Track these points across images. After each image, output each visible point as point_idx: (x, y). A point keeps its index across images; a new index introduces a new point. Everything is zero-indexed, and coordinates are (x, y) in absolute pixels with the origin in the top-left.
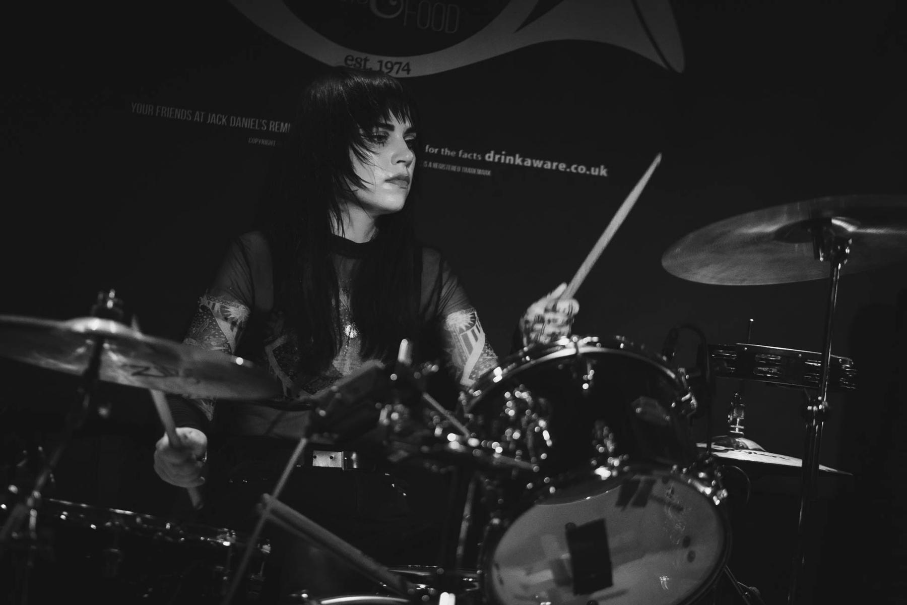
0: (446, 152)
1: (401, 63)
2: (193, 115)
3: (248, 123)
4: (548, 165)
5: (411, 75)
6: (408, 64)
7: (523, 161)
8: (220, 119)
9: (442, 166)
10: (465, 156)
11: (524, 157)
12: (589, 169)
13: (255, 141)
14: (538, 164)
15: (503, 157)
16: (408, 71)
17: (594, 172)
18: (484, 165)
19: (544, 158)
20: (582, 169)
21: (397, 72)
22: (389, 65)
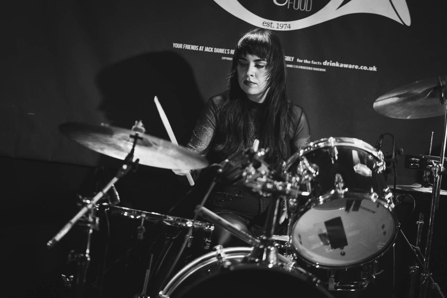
0: (306, 61)
2: (199, 48)
3: (221, 51)
4: (350, 66)
8: (210, 50)
9: (304, 68)
10: (315, 63)
11: (340, 63)
12: (368, 68)
13: (224, 58)
15: (331, 63)
16: (290, 27)
17: (371, 69)
18: (322, 67)
19: (348, 63)
20: (365, 68)
22: (282, 25)
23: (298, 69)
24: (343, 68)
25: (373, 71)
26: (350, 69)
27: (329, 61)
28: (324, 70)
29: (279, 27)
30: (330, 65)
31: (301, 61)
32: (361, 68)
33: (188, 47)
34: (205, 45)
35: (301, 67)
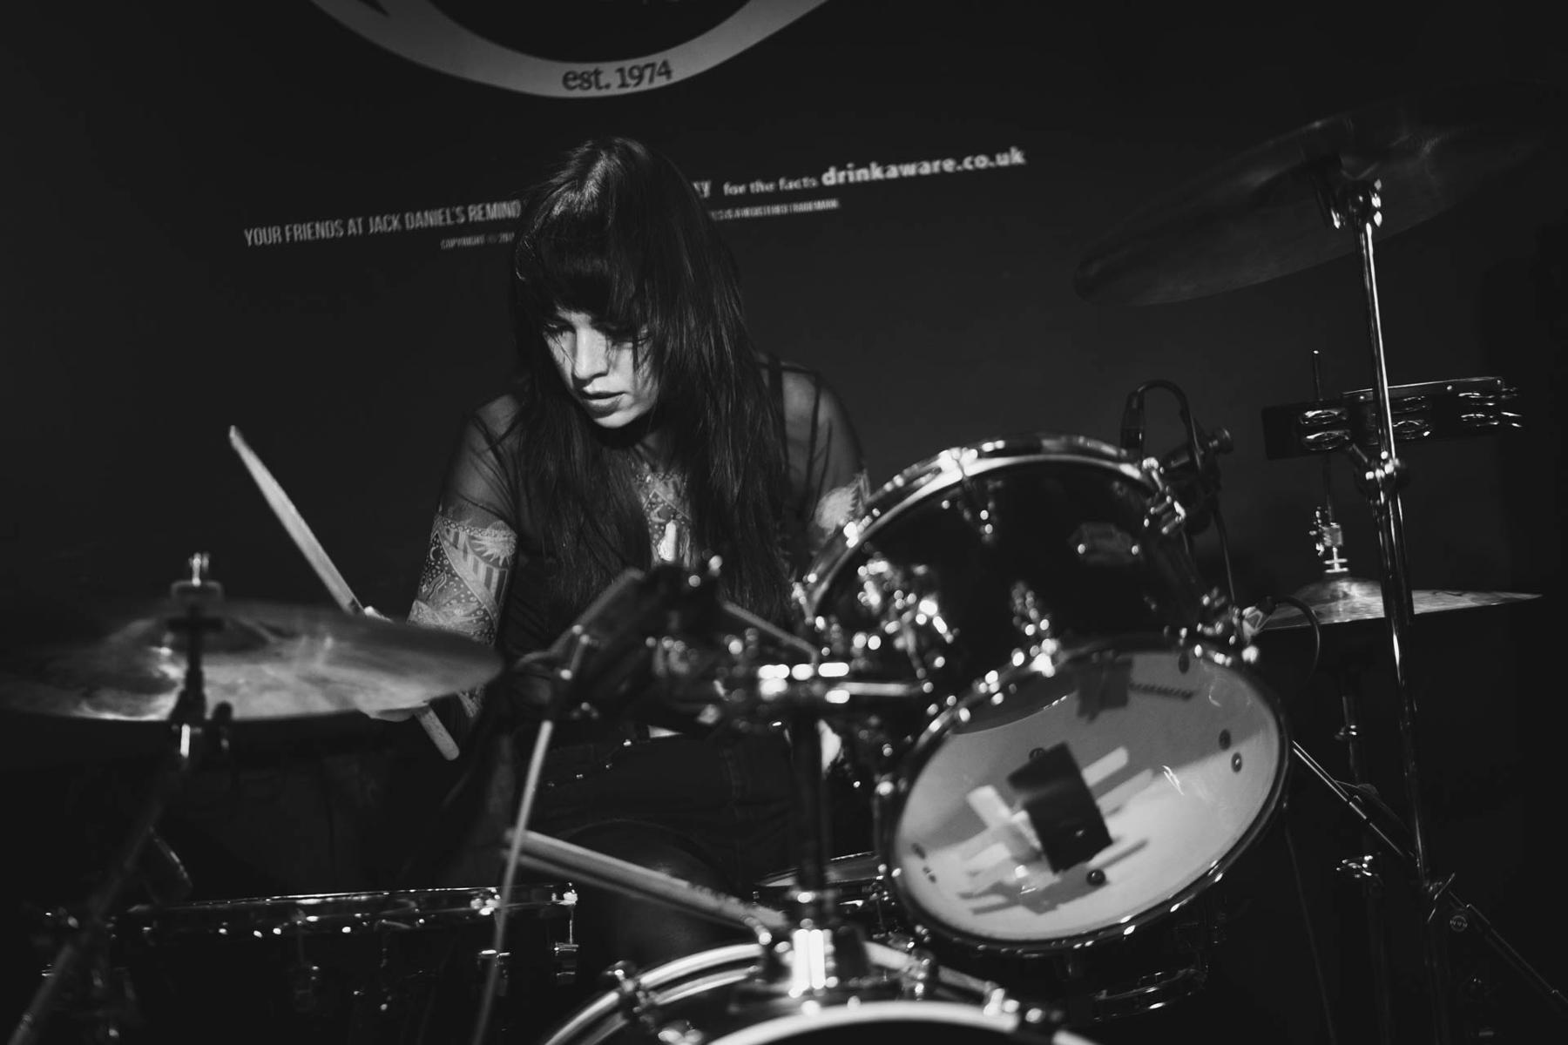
0: (758, 187)
1: (653, 65)
2: (345, 226)
3: (433, 218)
4: (926, 169)
5: (672, 81)
6: (665, 64)
7: (885, 171)
8: (390, 223)
9: (757, 212)
10: (793, 185)
11: (884, 164)
12: (993, 159)
13: (451, 243)
14: (909, 170)
15: (851, 174)
16: (668, 73)
17: (1003, 160)
18: (823, 192)
20: (982, 162)
21: (651, 80)
22: (636, 73)
23: (735, 220)
24: (901, 179)
25: (1013, 168)
26: (926, 177)
29: (629, 81)
30: (851, 179)
32: (967, 164)
33: (303, 232)
34: (367, 213)
35: (746, 212)
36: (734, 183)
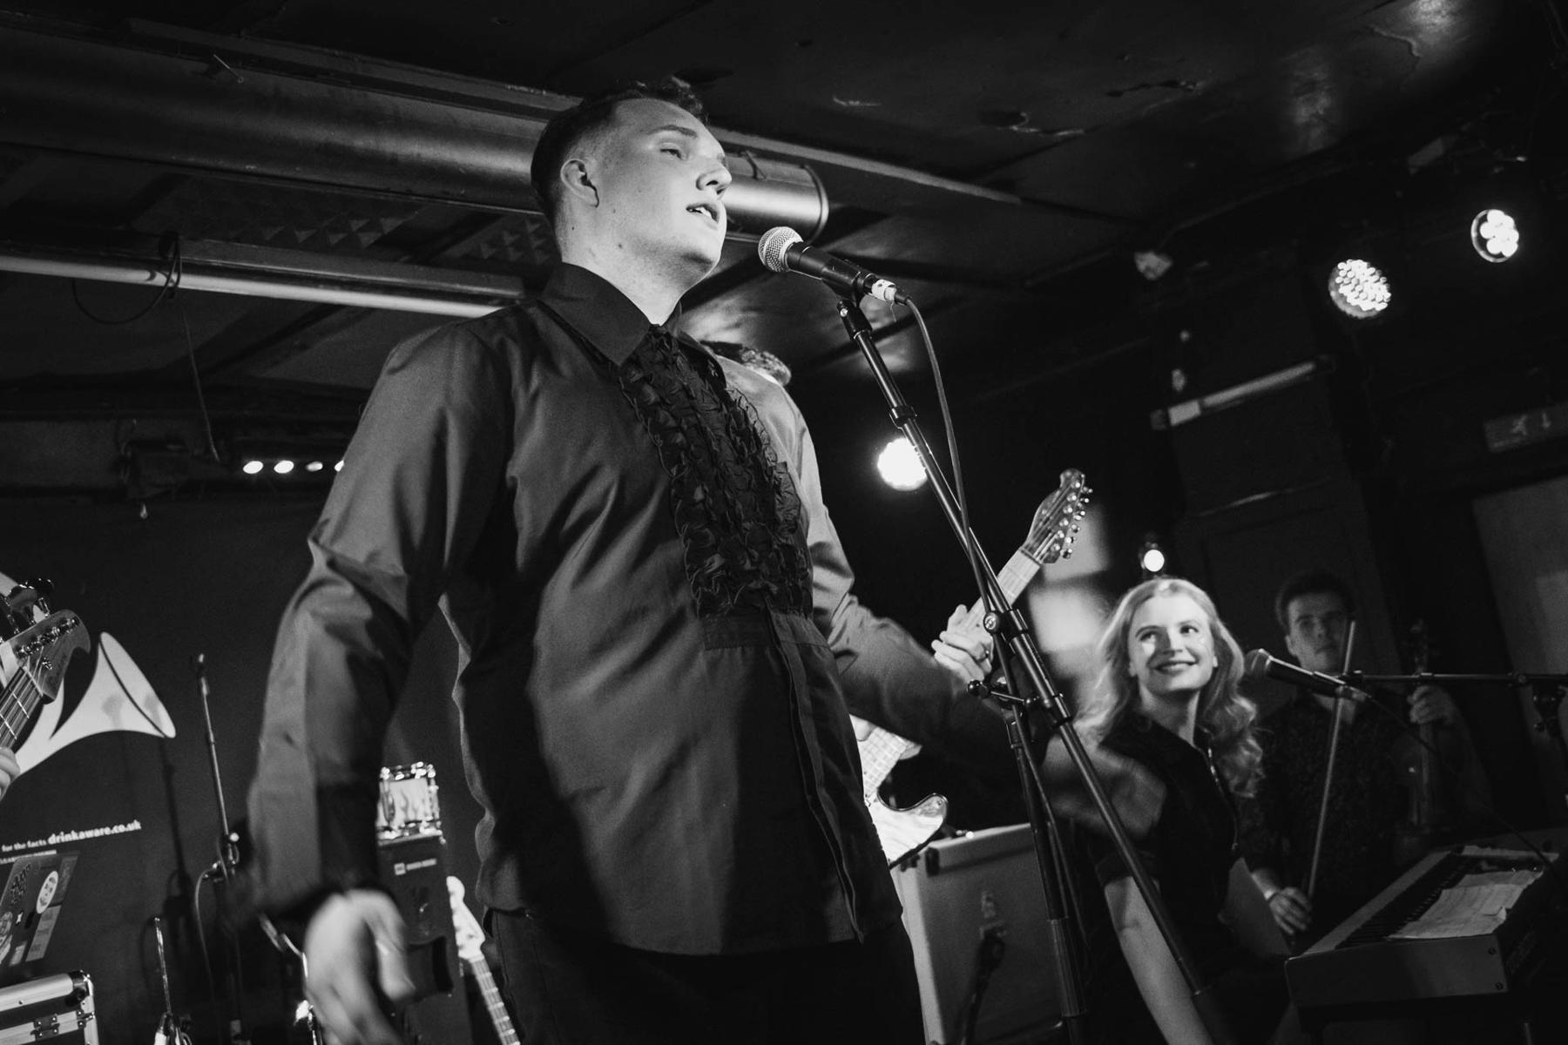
0: (18, 846)
10: (34, 845)
11: (78, 831)
18: (49, 847)
25: (135, 832)
27: (57, 834)
28: (54, 852)
31: (9, 848)
36: (8, 844)
